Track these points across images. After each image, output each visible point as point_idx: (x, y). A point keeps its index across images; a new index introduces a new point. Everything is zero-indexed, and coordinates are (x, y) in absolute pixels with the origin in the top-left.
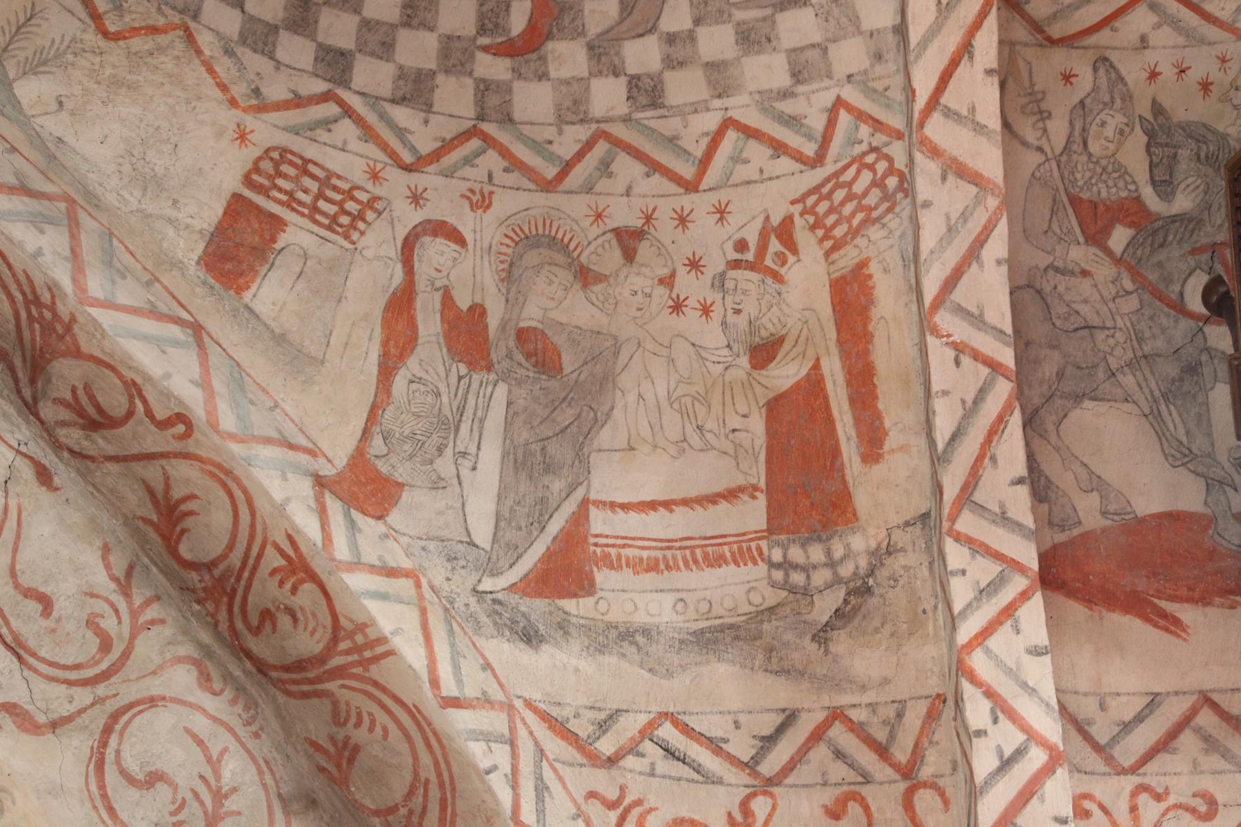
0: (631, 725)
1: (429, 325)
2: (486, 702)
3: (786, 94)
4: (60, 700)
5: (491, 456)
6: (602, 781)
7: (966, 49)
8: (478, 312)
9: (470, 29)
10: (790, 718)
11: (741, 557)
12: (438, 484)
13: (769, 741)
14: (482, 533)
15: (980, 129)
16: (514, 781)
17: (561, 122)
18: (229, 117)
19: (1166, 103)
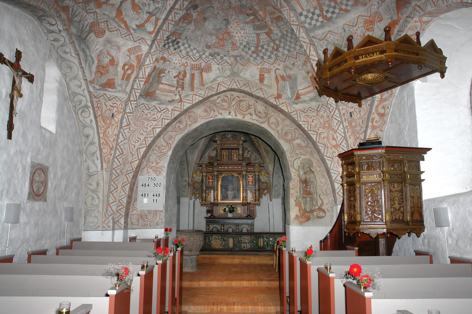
0: (307, 109)
1: (279, 78)
2: (294, 111)
3: (300, 49)
4: (264, 120)
5: (289, 89)
6: (305, 114)
7: (310, 50)
8: (283, 75)
9: (272, 50)
10: (319, 105)
11: (312, 92)
12: (285, 93)
13: (318, 108)
14: (290, 97)
15: (314, 56)
16: (297, 118)
17: (283, 56)
18: (256, 67)
19: (334, 42)
